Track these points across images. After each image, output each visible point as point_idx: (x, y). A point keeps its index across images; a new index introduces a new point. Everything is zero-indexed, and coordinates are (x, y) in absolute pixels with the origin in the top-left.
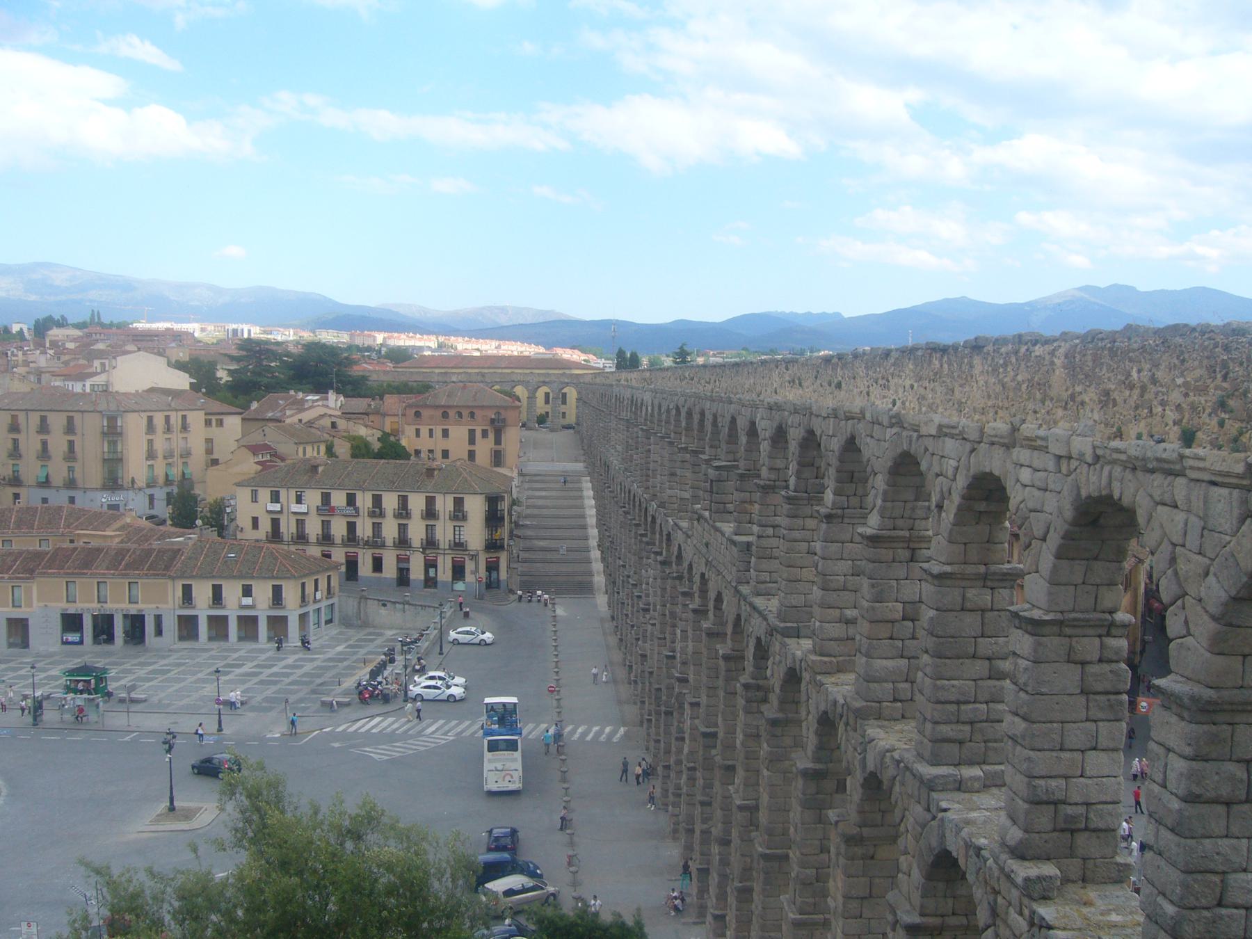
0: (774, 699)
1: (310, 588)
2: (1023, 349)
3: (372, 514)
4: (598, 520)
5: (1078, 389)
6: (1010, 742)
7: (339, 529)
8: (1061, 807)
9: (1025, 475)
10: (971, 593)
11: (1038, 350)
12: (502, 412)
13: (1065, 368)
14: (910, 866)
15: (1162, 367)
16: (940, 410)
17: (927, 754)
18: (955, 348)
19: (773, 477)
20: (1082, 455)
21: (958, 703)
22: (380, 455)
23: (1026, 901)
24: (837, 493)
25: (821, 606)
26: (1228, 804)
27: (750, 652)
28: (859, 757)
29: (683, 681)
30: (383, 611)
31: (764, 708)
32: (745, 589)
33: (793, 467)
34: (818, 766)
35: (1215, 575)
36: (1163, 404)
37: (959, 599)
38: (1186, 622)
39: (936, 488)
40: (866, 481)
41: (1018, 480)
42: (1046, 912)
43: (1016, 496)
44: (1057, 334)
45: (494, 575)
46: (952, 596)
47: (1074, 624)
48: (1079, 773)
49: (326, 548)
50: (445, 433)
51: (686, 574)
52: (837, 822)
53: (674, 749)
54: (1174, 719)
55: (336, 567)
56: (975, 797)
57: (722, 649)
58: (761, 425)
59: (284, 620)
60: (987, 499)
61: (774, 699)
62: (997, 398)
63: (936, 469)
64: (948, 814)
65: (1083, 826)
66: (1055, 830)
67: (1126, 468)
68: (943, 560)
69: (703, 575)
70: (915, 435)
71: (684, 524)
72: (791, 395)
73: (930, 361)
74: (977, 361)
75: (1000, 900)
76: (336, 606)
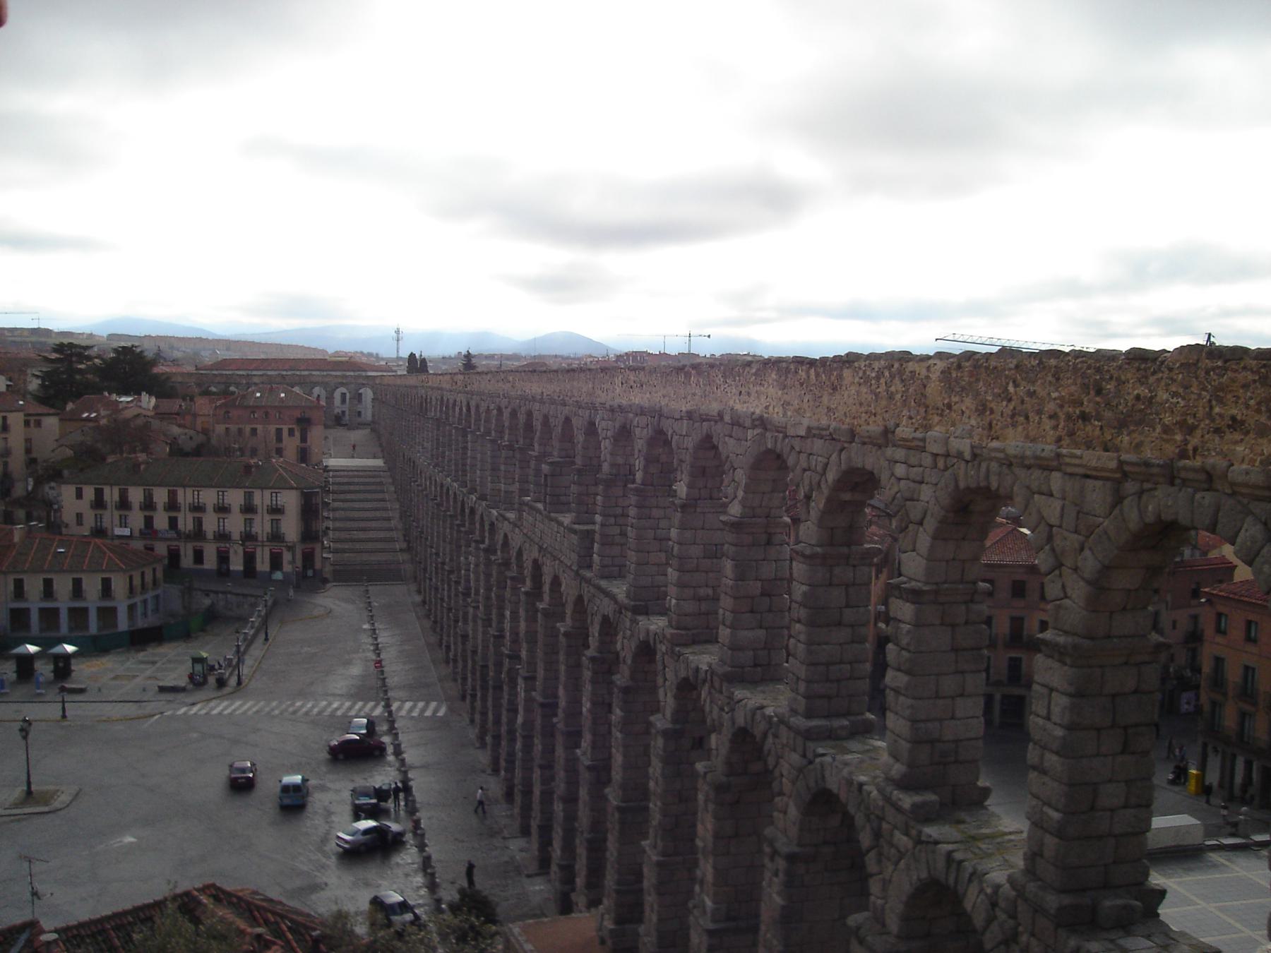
5: (955, 399)
6: (892, 693)
9: (900, 470)
10: (837, 570)
19: (614, 471)
26: (1098, 730)
34: (678, 727)
35: (1090, 549)
36: (1039, 412)
38: (1063, 587)
41: (893, 474)
49: (149, 542)
52: (705, 774)
54: (1056, 665)
56: (845, 744)
58: (601, 425)
59: (113, 611)
63: (805, 465)
68: (813, 542)
69: (535, 561)
72: (638, 398)
75: (885, 826)
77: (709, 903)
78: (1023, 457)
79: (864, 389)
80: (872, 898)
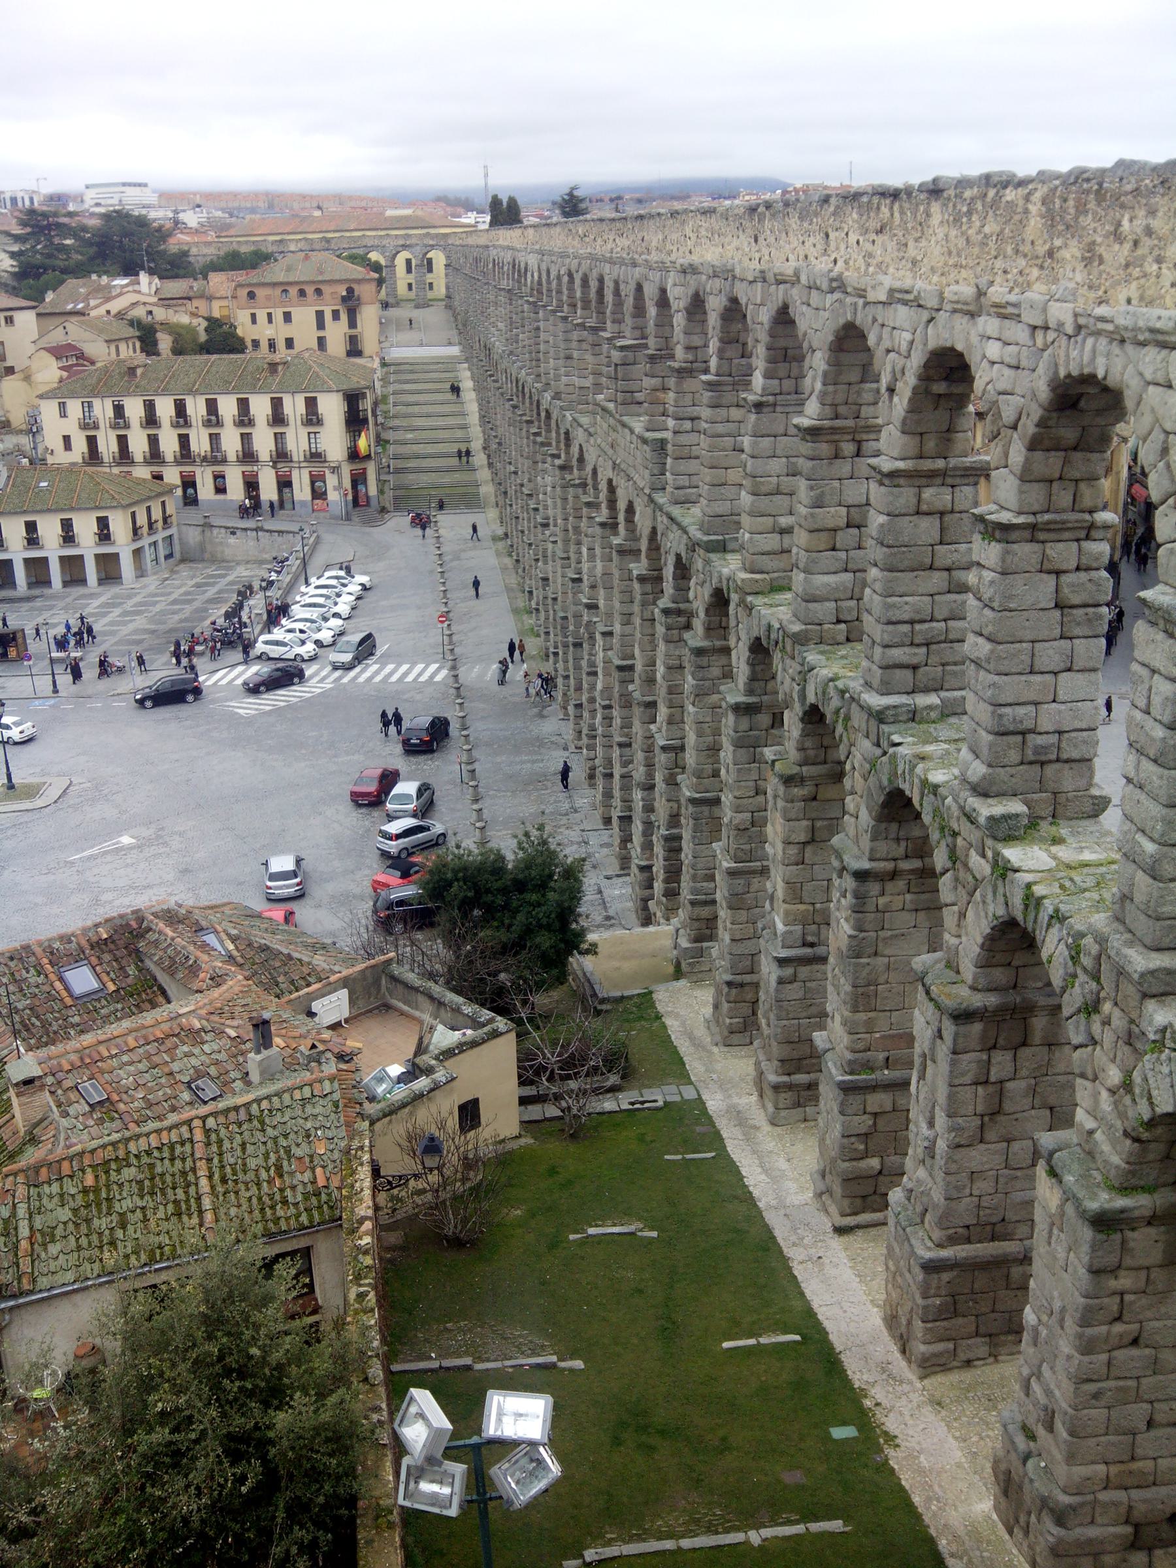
0: (698, 624)
1: (142, 520)
2: (992, 193)
3: (207, 423)
4: (482, 417)
5: (1058, 242)
6: (973, 666)
7: (169, 444)
8: (1030, 737)
9: (993, 350)
10: (927, 493)
11: (1010, 195)
12: (355, 286)
13: (1042, 217)
14: (858, 807)
15: (1160, 214)
16: (891, 270)
17: (876, 682)
18: (908, 191)
19: (690, 357)
20: (1061, 325)
21: (912, 622)
22: (206, 349)
23: (989, 842)
24: (768, 375)
25: (751, 514)
27: (669, 572)
28: (797, 688)
29: (593, 607)
30: (232, 540)
31: (687, 635)
32: (661, 499)
33: (714, 345)
36: (1159, 260)
37: (915, 500)
39: (885, 368)
40: (801, 359)
42: (1013, 854)
43: (983, 377)
44: (1034, 173)
45: (361, 488)
46: (906, 496)
47: (1048, 527)
48: (1051, 698)
49: (156, 469)
50: (287, 317)
51: (589, 481)
52: (773, 762)
53: (585, 686)
54: (1161, 636)
55: (170, 490)
57: (639, 567)
58: (673, 293)
59: (115, 557)
60: (946, 379)
61: (698, 624)
62: (959, 255)
63: (886, 344)
64: (900, 749)
65: (1054, 757)
66: (1022, 763)
67: (1112, 340)
69: (610, 481)
70: (861, 302)
71: (585, 420)
72: (709, 255)
73: (878, 208)
74: (935, 208)
76: (176, 537)
77: (780, 927)
78: (1137, 329)
79: (953, 233)
80: (946, 936)
